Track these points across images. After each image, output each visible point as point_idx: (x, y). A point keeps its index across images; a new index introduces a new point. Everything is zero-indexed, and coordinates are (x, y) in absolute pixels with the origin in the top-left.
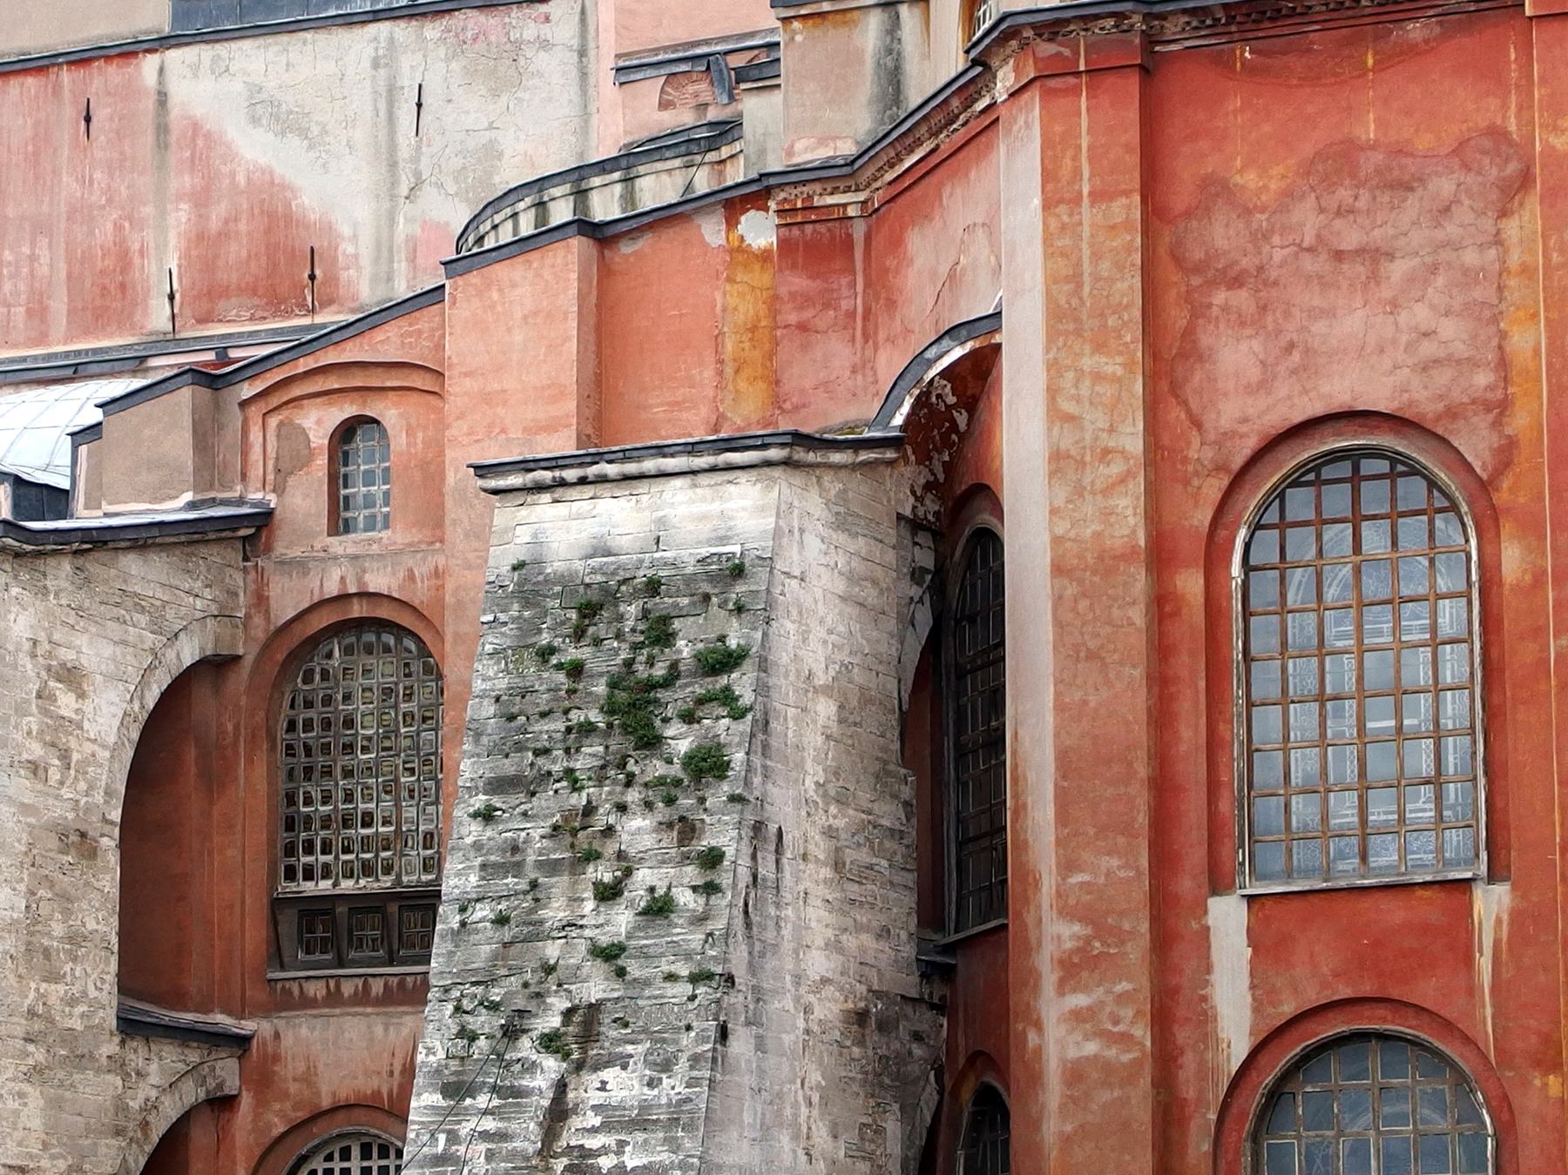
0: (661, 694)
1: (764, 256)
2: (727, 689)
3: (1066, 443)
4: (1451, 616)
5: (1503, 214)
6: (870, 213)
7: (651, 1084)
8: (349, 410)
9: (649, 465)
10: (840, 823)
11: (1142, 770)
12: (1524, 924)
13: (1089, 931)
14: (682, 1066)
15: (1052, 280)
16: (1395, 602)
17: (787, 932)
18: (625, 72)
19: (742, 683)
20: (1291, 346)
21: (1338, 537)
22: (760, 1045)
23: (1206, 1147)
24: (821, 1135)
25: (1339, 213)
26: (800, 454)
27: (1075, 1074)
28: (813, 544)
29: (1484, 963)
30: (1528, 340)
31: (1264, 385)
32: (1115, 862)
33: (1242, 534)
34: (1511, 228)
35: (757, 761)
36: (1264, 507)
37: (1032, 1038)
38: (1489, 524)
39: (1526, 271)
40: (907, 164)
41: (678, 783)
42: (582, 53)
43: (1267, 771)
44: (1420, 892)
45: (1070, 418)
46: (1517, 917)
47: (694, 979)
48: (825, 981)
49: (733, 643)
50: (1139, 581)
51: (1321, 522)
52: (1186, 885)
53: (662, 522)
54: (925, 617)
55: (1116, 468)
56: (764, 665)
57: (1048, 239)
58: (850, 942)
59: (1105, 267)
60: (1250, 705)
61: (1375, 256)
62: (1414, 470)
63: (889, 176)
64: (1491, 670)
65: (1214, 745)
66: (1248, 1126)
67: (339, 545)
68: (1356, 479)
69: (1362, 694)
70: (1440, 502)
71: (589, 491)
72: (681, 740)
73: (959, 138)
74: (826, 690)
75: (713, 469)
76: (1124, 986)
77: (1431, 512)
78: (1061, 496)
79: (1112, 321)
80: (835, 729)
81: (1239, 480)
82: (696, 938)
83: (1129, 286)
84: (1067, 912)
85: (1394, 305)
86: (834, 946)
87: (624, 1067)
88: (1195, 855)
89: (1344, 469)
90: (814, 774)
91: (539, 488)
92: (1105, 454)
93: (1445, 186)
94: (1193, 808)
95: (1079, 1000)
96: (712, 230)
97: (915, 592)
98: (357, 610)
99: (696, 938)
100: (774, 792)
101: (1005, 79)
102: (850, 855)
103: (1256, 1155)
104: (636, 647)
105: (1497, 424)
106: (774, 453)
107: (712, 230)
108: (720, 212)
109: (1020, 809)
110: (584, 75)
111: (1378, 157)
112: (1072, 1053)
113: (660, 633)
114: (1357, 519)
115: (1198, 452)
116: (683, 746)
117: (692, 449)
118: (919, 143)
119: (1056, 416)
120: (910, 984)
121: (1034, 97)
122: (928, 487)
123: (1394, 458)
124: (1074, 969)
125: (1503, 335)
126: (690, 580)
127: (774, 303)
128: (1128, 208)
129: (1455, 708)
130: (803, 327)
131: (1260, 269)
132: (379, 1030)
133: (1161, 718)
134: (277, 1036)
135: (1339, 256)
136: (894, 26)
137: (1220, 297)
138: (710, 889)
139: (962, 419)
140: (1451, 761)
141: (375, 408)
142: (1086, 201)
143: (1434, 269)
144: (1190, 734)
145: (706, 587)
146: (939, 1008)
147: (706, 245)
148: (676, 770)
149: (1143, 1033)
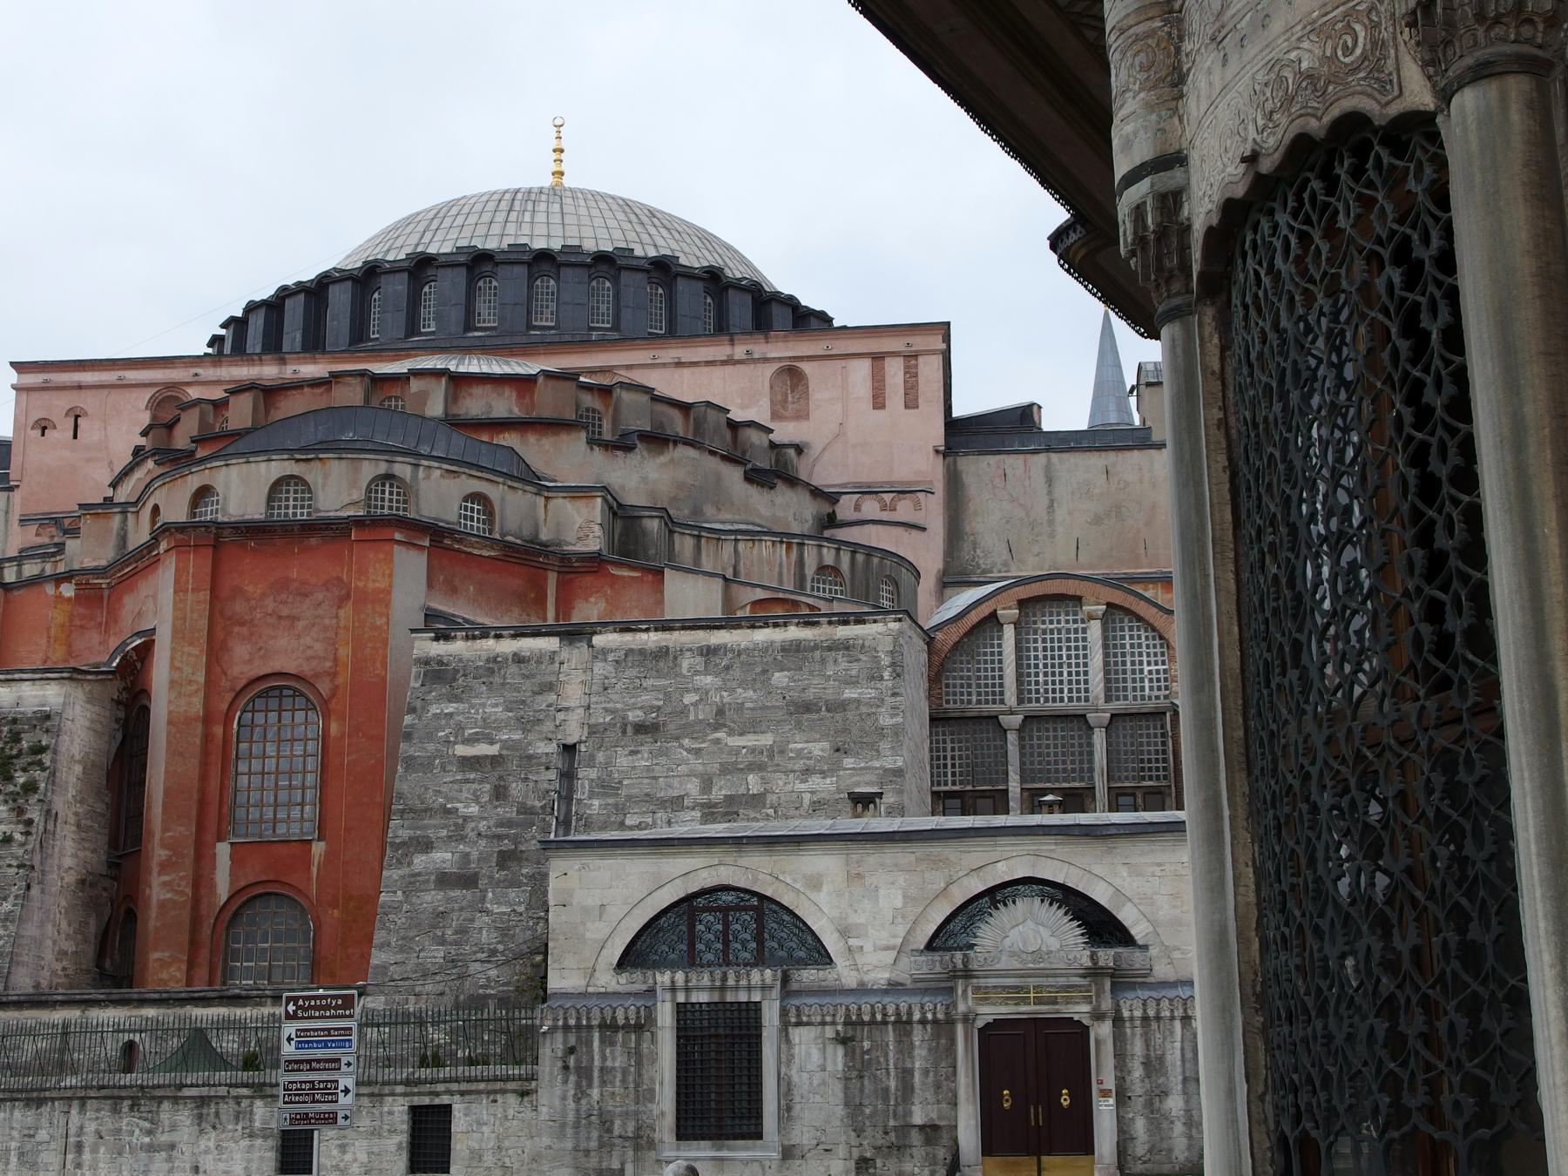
0: (15, 761)
1: (69, 599)
2: (40, 760)
3: (176, 676)
4: (311, 746)
5: (339, 607)
6: (110, 586)
9: (17, 676)
10: (81, 810)
11: (195, 796)
12: (329, 855)
14: (11, 899)
15: (175, 619)
16: (292, 740)
17: (56, 849)
18: (23, 521)
19: (46, 759)
21: (273, 716)
22: (43, 891)
23: (209, 932)
24: (64, 925)
26: (75, 676)
27: (162, 904)
28: (78, 708)
29: (314, 870)
30: (345, 652)
31: (250, 661)
32: (182, 829)
33: (238, 713)
34: (342, 613)
35: (50, 787)
36: (247, 704)
37: (148, 891)
38: (327, 717)
39: (346, 628)
41: (18, 793)
42: (7, 513)
43: (241, 798)
45: (178, 668)
46: (327, 853)
47: (19, 867)
48: (70, 868)
49: (44, 743)
50: (199, 728)
51: (267, 711)
52: (209, 838)
53: (20, 697)
54: (119, 736)
55: (194, 688)
56: (55, 752)
57: (175, 603)
58: (81, 854)
59: (195, 616)
60: (237, 774)
61: (293, 619)
62: (302, 694)
64: (324, 766)
65: (222, 788)
66: (225, 924)
68: (281, 697)
69: (277, 772)
70: (310, 706)
72: (21, 779)
73: (147, 563)
74: (79, 762)
75: (41, 679)
76: (183, 873)
77: (306, 710)
78: (173, 698)
79: (196, 635)
80: (81, 776)
81: (238, 694)
82: (21, 852)
83: (204, 623)
84: (164, 846)
85: (299, 636)
86: (75, 856)
88: (213, 828)
89: (277, 693)
90: (72, 792)
93: (320, 596)
94: (213, 810)
95: (166, 878)
96: (50, 589)
97: (117, 726)
99: (21, 852)
100: (55, 798)
101: (163, 546)
102: (83, 822)
103: (227, 935)
104: (6, 743)
105: (332, 681)
106: (65, 675)
107: (50, 589)
108: (53, 583)
109: (149, 808)
110: (7, 521)
111: (296, 584)
112: (162, 897)
113: (16, 738)
114: (280, 711)
115: (224, 683)
116: (22, 780)
117: (34, 671)
118: (130, 564)
119: (173, 667)
120: (103, 870)
121: (174, 551)
122: (124, 689)
123: (295, 690)
124: (165, 867)
125: (336, 649)
126: (29, 719)
127: (71, 617)
128: (205, 595)
129: (310, 779)
130: (82, 627)
131: (252, 620)
133: (204, 777)
135: (280, 617)
136: (125, 520)
137: (236, 629)
138: (28, 833)
139: (139, 665)
140: (308, 798)
143: (314, 625)
144: (214, 783)
145: (35, 722)
146: (114, 879)
147: (46, 594)
148: (18, 789)
149: (189, 891)
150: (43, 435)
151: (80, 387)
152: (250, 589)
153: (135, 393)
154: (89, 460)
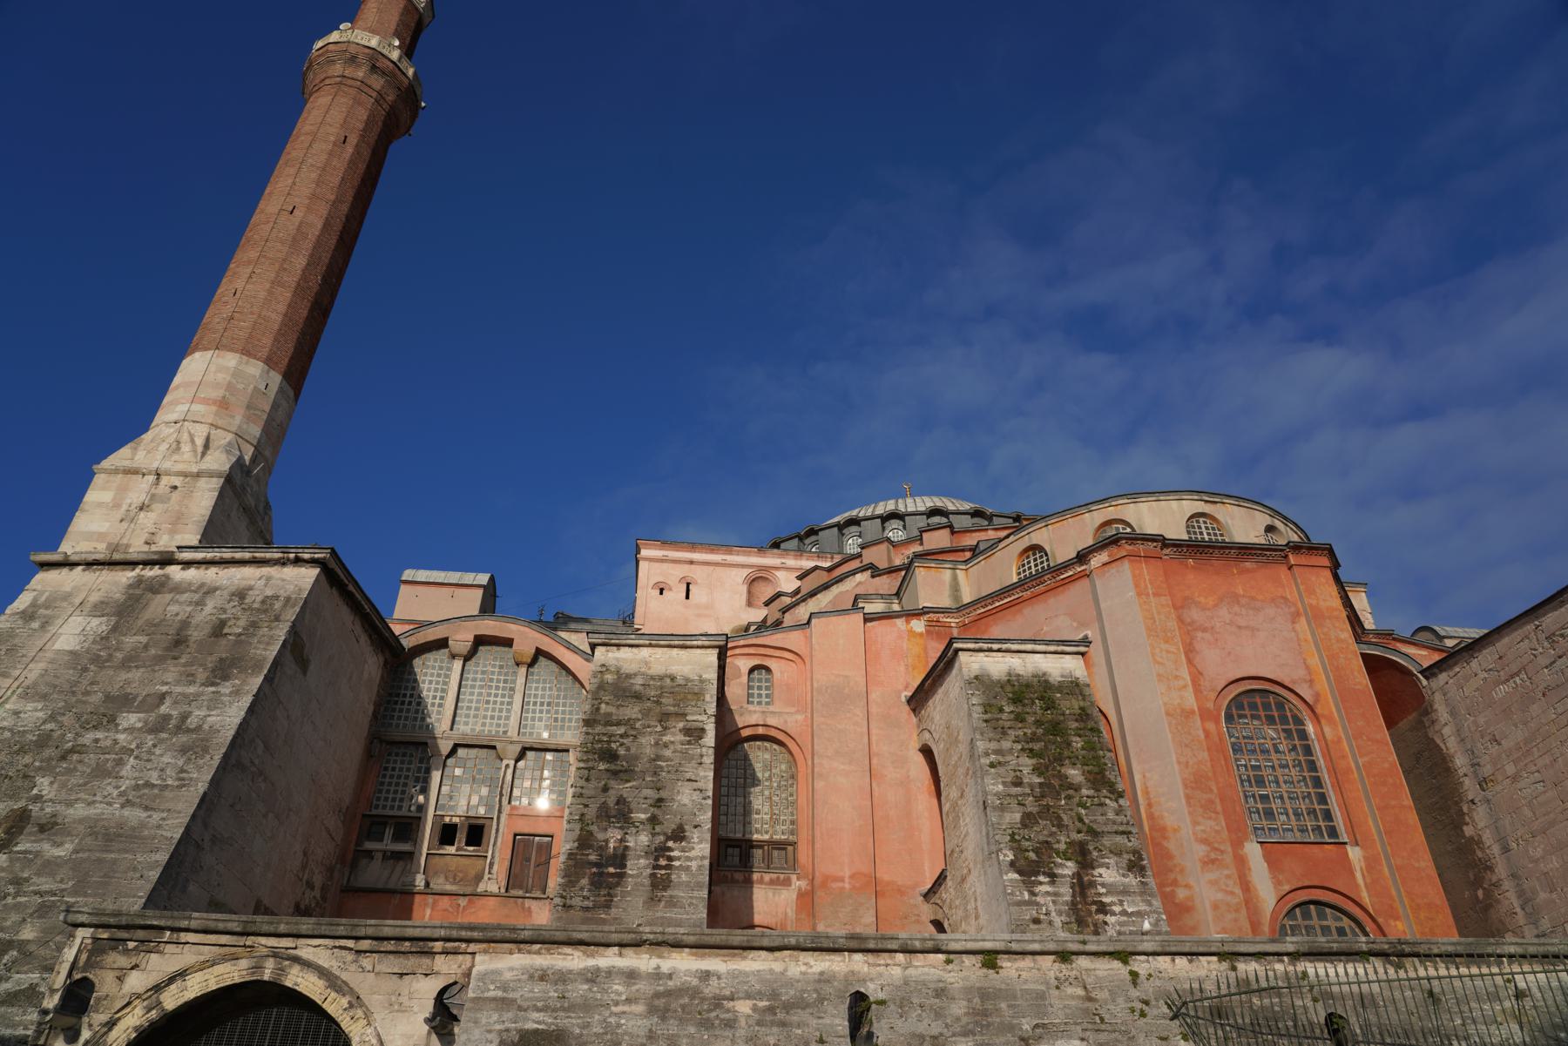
1: (921, 635)
5: (1294, 622)
7: (1124, 876)
8: (756, 661)
9: (1029, 647)
12: (1371, 864)
13: (1208, 848)
20: (1229, 653)
25: (1236, 614)
29: (1358, 875)
34: (1297, 626)
40: (997, 604)
44: (1326, 846)
55: (1181, 683)
63: (983, 610)
67: (751, 707)
71: (1000, 654)
87: (1108, 868)
91: (981, 650)
92: (1177, 677)
98: (761, 731)
124: (1208, 863)
125: (1305, 660)
131: (1212, 628)
132: (770, 895)
134: (723, 894)
135: (1239, 627)
141: (767, 662)
142: (1151, 596)
149: (1238, 890)
150: (661, 593)
151: (692, 562)
152: (1202, 599)
153: (734, 571)
154: (699, 616)
